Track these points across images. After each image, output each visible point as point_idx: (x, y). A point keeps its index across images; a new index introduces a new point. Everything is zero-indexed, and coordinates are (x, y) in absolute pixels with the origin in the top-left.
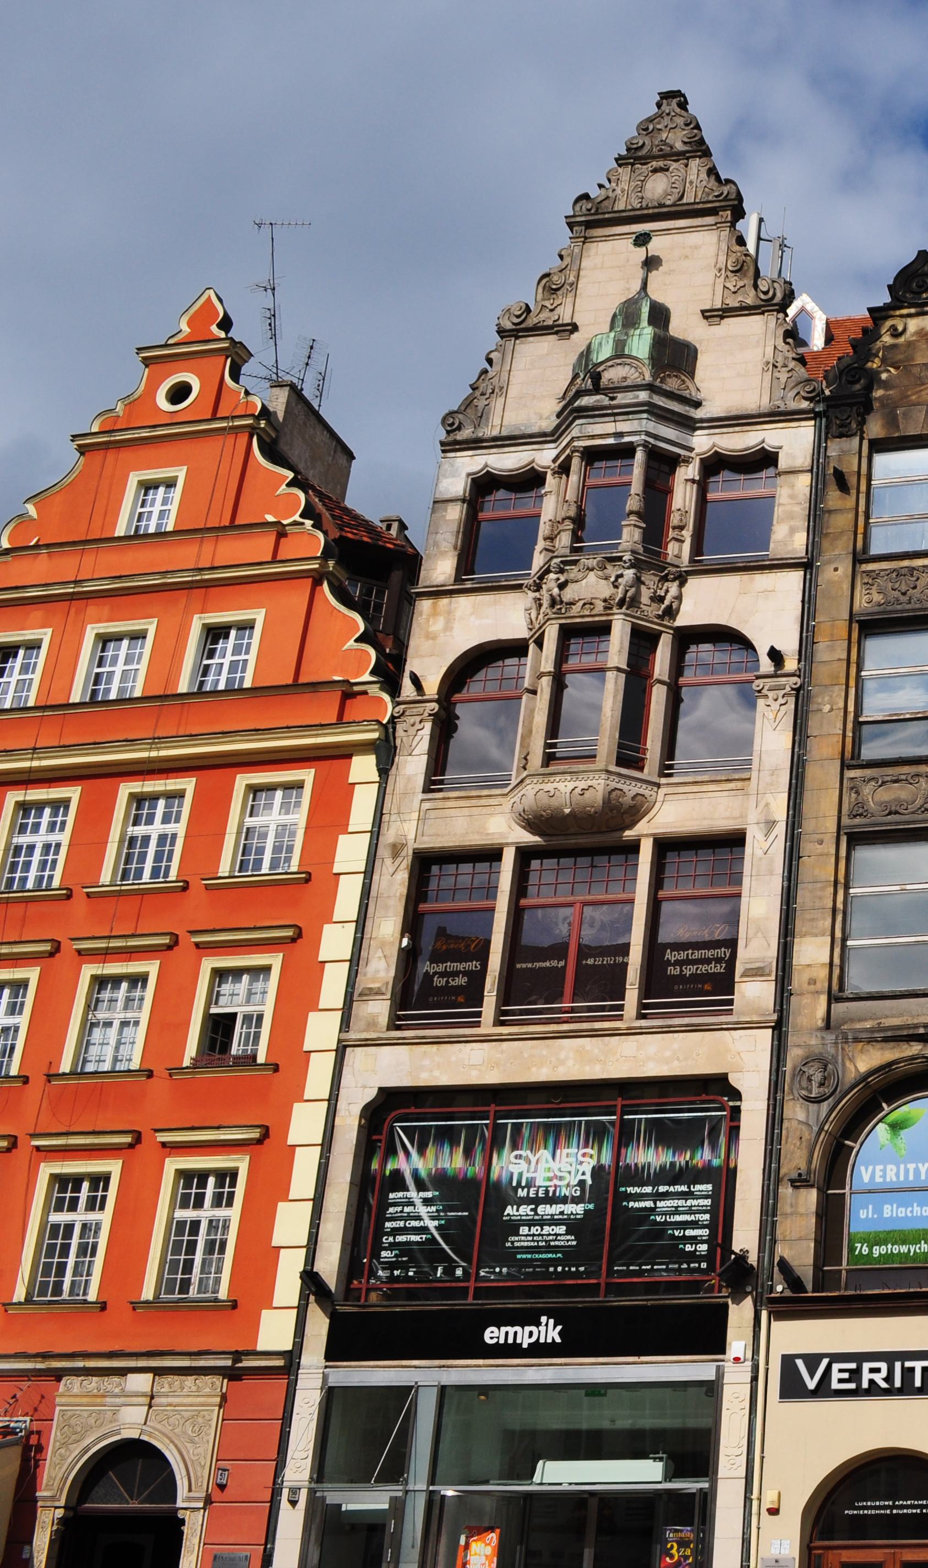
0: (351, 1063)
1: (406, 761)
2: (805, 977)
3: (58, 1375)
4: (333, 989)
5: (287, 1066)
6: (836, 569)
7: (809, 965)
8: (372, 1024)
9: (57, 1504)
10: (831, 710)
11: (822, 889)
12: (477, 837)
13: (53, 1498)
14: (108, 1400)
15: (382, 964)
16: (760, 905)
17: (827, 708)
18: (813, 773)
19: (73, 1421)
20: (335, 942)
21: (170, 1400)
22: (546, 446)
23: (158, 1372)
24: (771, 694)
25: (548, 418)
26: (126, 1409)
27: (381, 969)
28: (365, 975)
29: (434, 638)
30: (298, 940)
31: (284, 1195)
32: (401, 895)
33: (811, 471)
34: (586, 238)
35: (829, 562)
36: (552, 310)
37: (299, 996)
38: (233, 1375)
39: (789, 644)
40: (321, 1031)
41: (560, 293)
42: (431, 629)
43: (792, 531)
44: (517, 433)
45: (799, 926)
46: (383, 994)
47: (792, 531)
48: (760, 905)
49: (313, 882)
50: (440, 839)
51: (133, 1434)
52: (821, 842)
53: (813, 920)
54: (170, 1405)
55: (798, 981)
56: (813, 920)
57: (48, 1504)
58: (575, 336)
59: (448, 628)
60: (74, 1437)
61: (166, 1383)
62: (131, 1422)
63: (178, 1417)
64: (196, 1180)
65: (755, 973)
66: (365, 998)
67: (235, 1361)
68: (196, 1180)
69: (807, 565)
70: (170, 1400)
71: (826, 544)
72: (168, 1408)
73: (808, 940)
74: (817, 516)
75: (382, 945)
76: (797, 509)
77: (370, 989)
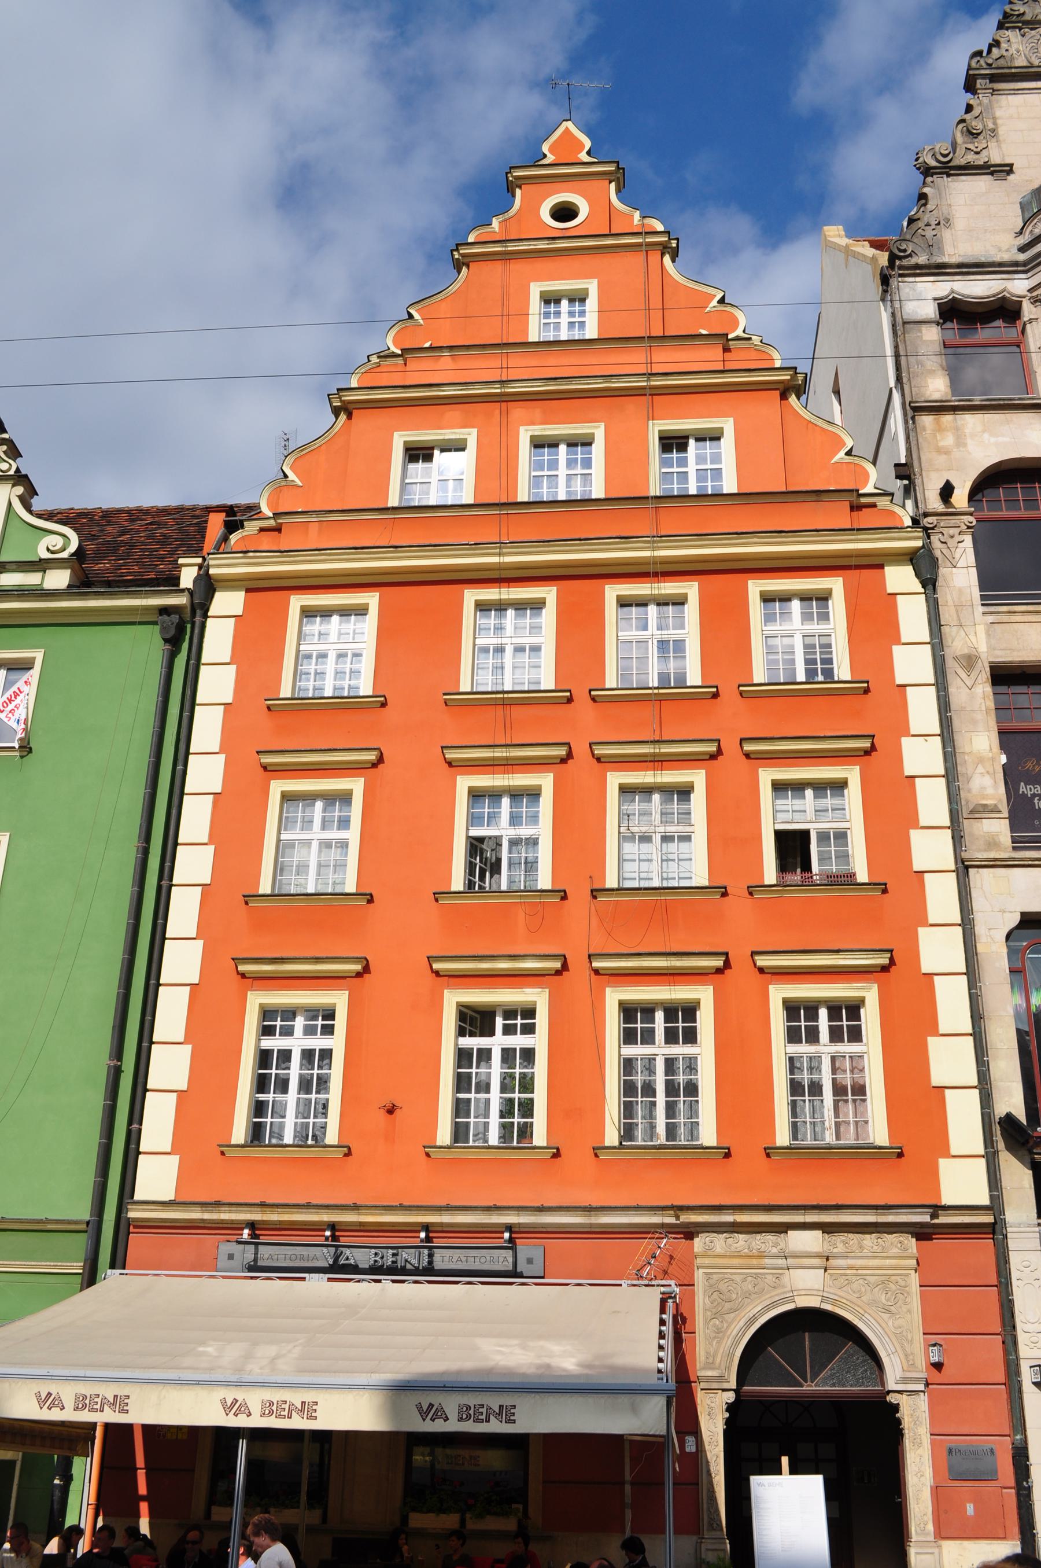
0: (979, 885)
1: (951, 573)
3: (689, 1233)
4: (932, 802)
5: (894, 888)
8: (992, 843)
9: (726, 1386)
12: (999, 653)
13: (720, 1378)
14: (767, 1262)
15: (987, 781)
19: (723, 1286)
20: (921, 756)
21: (850, 1262)
22: (1016, 276)
23: (828, 1228)
25: (1008, 250)
26: (805, 1274)
27: (987, 783)
28: (969, 791)
29: (947, 452)
30: (873, 752)
31: (932, 1028)
32: (987, 711)
34: (994, 90)
36: (977, 153)
37: (892, 811)
38: (922, 1233)
40: (931, 850)
41: (981, 137)
42: (941, 444)
44: (983, 260)
46: (1000, 812)
49: (873, 691)
50: (1015, 653)
51: (813, 1302)
54: (851, 1268)
57: (715, 1385)
58: (1011, 177)
59: (960, 442)
60: (728, 1306)
61: (840, 1242)
62: (807, 1289)
63: (861, 1281)
64: (844, 1011)
66: (977, 816)
67: (934, 1216)
68: (844, 1011)
70: (850, 1262)
72: (848, 1272)
75: (981, 760)
77: (985, 806)
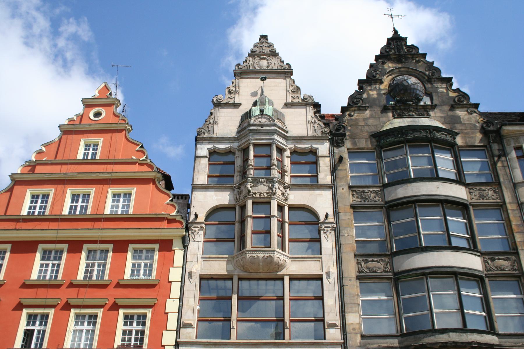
2: (351, 327)
6: (343, 189)
7: (352, 323)
10: (348, 235)
11: (353, 297)
16: (331, 300)
17: (346, 235)
18: (344, 256)
24: (326, 229)
33: (330, 157)
35: (340, 186)
39: (331, 213)
43: (326, 175)
45: (346, 310)
47: (326, 175)
48: (331, 300)
52: (350, 280)
53: (351, 307)
55: (349, 329)
56: (351, 307)
65: (333, 326)
69: (332, 187)
71: (338, 180)
73: (350, 314)
74: (333, 172)
76: (326, 168)
